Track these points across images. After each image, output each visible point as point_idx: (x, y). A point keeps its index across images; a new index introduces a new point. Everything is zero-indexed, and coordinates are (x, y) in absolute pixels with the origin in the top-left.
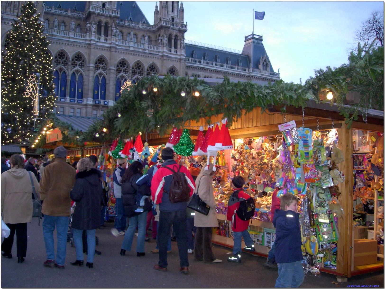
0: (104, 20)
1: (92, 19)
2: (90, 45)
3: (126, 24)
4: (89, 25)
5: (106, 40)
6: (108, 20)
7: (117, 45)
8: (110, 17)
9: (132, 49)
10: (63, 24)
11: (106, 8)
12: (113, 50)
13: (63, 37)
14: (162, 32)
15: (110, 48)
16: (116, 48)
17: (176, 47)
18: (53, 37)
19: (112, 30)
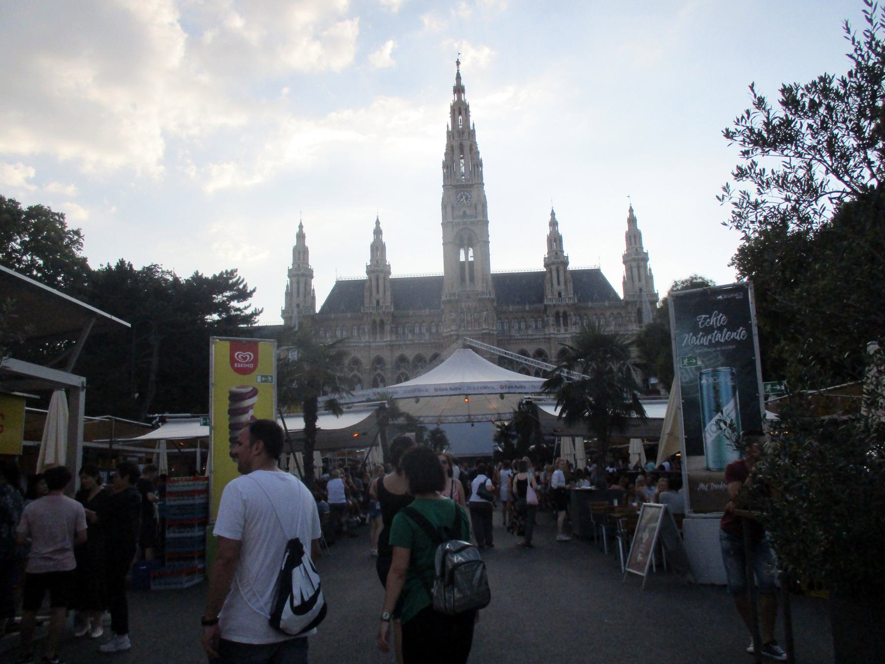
0: (561, 310)
1: (548, 313)
2: (549, 339)
4: (546, 319)
5: (566, 330)
8: (567, 304)
10: (523, 320)
11: (563, 297)
13: (522, 335)
19: (571, 319)
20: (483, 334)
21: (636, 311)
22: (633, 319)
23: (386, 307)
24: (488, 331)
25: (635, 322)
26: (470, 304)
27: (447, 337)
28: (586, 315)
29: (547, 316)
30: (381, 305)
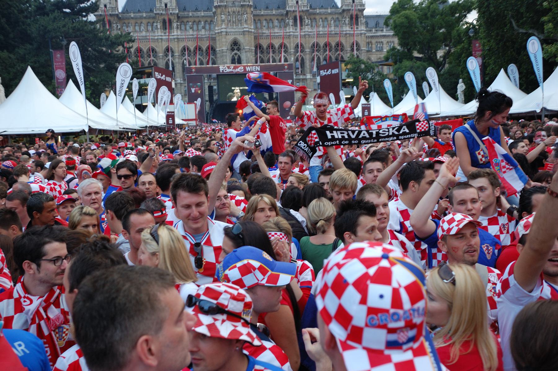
1: (289, 16)
2: (289, 35)
3: (318, 12)
4: (287, 21)
6: (301, 13)
7: (310, 32)
8: (302, 11)
9: (321, 33)
10: (271, 21)
12: (307, 36)
14: (345, 14)
15: (305, 35)
16: (309, 35)
17: (357, 24)
18: (264, 35)
19: (305, 21)
20: (244, 31)
21: (349, 16)
22: (347, 22)
23: (173, 9)
24: (247, 29)
25: (349, 24)
26: (235, 9)
27: (218, 33)
28: (315, 19)
29: (289, 19)
30: (168, 7)
